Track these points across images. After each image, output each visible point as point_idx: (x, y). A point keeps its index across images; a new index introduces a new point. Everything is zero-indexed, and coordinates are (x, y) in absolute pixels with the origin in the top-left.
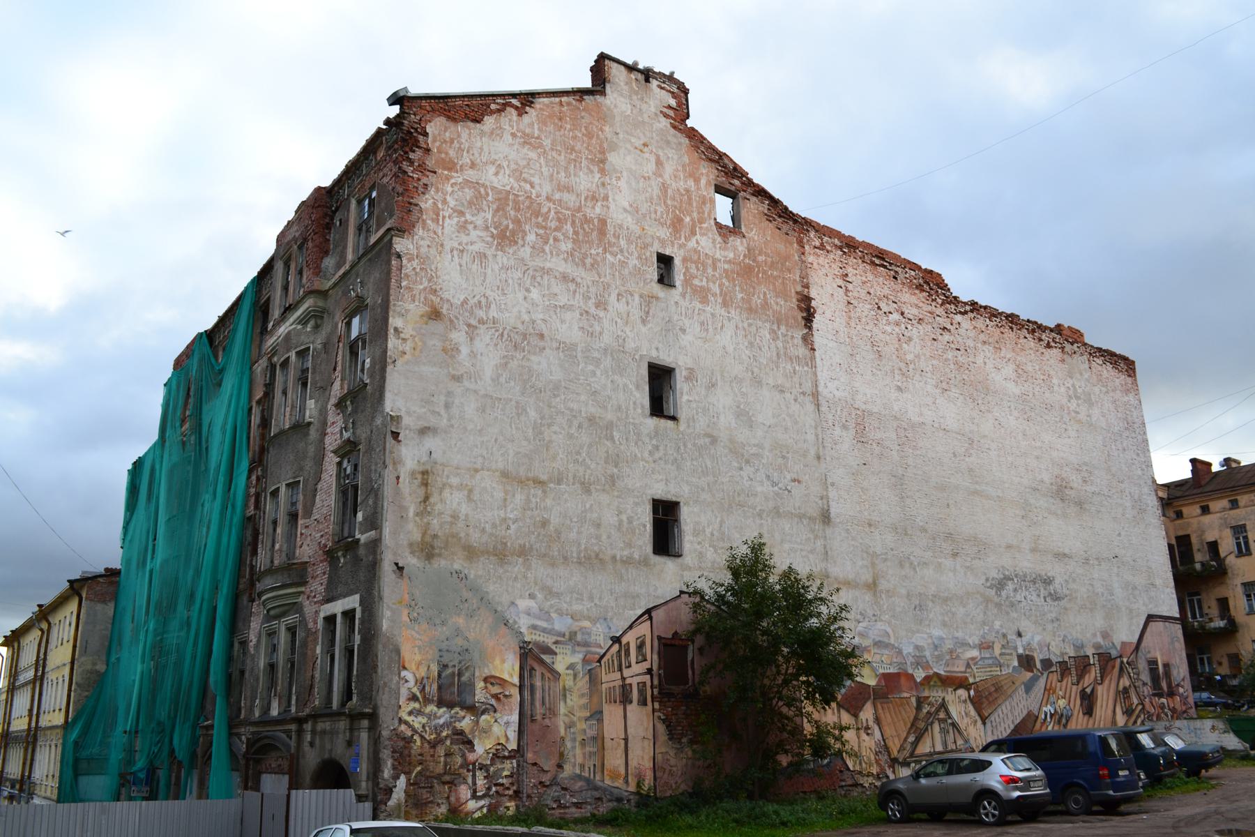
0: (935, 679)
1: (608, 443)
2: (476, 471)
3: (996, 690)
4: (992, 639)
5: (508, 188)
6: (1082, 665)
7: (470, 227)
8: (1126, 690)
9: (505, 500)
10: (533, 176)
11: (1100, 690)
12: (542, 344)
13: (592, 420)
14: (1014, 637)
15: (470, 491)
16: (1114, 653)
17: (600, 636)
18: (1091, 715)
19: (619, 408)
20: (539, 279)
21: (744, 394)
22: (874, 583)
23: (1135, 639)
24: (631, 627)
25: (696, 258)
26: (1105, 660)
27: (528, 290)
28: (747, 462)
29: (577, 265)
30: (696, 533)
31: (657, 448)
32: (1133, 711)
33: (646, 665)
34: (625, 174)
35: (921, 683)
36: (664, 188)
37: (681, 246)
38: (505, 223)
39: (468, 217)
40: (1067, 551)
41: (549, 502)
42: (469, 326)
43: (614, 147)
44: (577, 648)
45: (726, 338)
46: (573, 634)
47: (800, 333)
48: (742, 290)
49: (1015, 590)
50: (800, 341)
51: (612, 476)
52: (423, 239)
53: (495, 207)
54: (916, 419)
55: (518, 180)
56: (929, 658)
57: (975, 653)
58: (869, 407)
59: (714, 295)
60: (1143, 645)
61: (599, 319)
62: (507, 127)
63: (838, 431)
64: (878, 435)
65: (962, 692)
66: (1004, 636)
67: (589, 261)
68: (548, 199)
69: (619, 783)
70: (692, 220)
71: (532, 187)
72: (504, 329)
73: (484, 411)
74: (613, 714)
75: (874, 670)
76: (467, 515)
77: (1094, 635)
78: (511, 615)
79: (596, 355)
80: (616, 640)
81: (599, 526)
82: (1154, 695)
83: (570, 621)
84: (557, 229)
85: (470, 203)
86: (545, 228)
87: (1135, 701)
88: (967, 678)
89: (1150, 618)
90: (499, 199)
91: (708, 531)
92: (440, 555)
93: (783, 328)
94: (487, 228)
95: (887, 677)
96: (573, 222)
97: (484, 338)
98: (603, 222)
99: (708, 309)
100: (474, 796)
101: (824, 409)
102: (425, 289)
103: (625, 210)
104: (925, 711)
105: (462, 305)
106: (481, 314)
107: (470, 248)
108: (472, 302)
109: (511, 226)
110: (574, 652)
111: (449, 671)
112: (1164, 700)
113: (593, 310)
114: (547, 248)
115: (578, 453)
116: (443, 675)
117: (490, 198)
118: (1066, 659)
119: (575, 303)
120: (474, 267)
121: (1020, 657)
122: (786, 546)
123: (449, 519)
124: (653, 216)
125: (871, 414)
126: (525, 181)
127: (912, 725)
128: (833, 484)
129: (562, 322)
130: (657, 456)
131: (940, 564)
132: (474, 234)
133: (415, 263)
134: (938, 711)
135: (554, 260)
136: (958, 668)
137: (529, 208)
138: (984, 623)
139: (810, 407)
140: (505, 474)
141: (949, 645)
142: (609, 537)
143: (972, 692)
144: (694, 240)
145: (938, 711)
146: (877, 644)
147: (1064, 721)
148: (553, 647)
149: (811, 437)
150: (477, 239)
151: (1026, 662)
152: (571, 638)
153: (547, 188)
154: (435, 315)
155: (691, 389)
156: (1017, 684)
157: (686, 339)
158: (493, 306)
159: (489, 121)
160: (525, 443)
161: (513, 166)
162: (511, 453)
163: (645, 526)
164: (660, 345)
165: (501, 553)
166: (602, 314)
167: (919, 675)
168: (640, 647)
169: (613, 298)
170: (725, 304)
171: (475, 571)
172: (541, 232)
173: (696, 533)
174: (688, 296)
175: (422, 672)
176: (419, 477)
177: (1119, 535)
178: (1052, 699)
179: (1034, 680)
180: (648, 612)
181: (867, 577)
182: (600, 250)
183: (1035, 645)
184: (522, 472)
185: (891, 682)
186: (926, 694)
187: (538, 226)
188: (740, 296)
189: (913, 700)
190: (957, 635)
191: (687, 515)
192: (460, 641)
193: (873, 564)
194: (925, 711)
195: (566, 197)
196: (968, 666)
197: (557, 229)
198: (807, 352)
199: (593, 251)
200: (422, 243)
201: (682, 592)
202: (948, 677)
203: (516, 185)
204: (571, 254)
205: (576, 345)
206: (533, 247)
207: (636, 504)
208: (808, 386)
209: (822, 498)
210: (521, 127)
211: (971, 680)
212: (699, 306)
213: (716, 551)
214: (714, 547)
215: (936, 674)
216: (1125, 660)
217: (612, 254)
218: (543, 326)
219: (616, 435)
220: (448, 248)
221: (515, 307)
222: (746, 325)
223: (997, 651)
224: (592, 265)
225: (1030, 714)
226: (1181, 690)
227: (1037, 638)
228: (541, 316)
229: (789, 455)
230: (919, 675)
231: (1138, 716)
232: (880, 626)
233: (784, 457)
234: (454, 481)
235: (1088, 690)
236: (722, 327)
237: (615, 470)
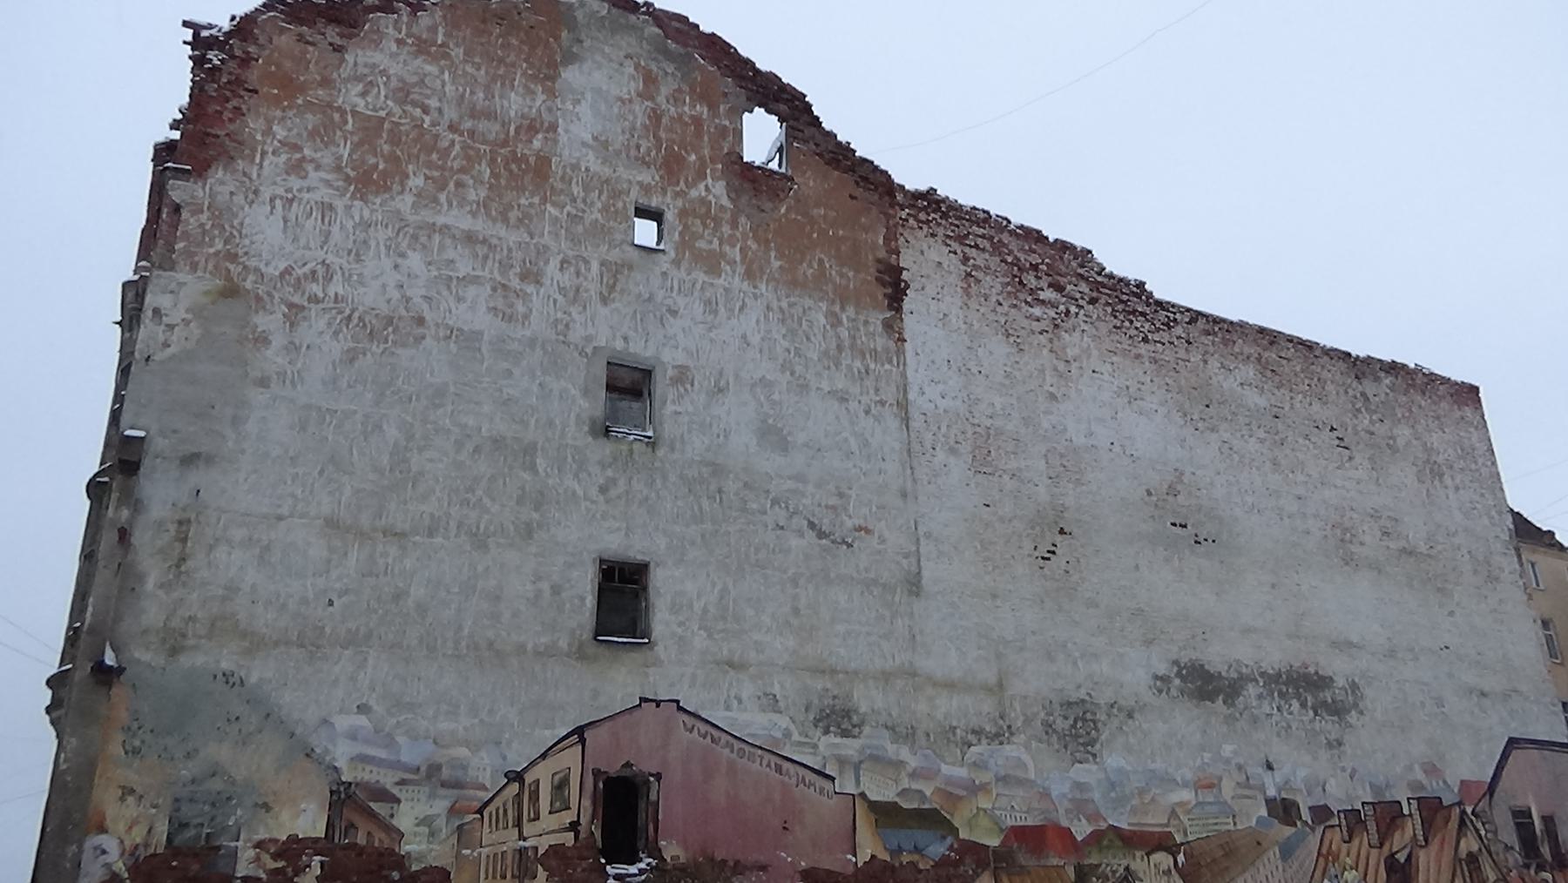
0: (1111, 835)
1: (526, 476)
2: (280, 518)
3: (1226, 855)
5: (383, 114)
6: (1388, 815)
7: (310, 168)
8: (1472, 858)
9: (329, 561)
10: (428, 97)
12: (421, 330)
13: (498, 442)
14: (1260, 770)
15: (267, 548)
17: (485, 769)
19: (551, 423)
20: (423, 239)
21: (774, 403)
22: (1000, 685)
24: (544, 756)
25: (703, 210)
27: (403, 255)
28: (775, 502)
29: (494, 220)
31: (614, 481)
33: (568, 817)
34: (589, 96)
36: (656, 116)
37: (677, 195)
38: (372, 161)
39: (307, 152)
41: (408, 563)
42: (291, 306)
43: (570, 58)
44: (443, 792)
45: (749, 322)
46: (434, 769)
47: (877, 318)
48: (780, 256)
49: (1260, 697)
50: (880, 329)
51: (528, 525)
52: (222, 183)
53: (356, 139)
54: (1080, 440)
55: (402, 102)
57: (1186, 795)
58: (998, 423)
59: (732, 263)
61: (524, 296)
62: (391, 31)
63: (941, 456)
64: (1013, 464)
65: (1162, 859)
66: (1240, 768)
67: (514, 215)
68: (452, 128)
70: (701, 159)
71: (426, 111)
72: (353, 311)
73: (303, 428)
76: (253, 586)
77: (1410, 768)
78: (319, 742)
79: (515, 346)
80: (516, 777)
81: (498, 598)
83: (429, 747)
84: (462, 170)
85: (313, 134)
86: (442, 168)
89: (1513, 743)
90: (366, 129)
91: (698, 606)
92: (196, 648)
93: (851, 311)
94: (338, 169)
96: (493, 161)
97: (316, 324)
98: (544, 162)
99: (721, 281)
101: (917, 423)
102: (217, 253)
103: (584, 144)
105: (282, 275)
106: (316, 289)
107: (306, 196)
108: (300, 272)
109: (381, 167)
110: (432, 796)
111: (191, 833)
113: (515, 283)
114: (443, 197)
115: (471, 490)
116: (177, 841)
117: (349, 127)
119: (486, 273)
120: (309, 224)
121: (1270, 802)
122: (840, 628)
123: (221, 592)
124: (633, 153)
125: (1000, 432)
126: (415, 104)
128: (928, 535)
129: (459, 299)
130: (613, 493)
132: (314, 176)
133: (204, 217)
135: (455, 212)
136: (1154, 821)
137: (415, 141)
139: (893, 423)
140: (332, 523)
142: (515, 615)
143: (1181, 858)
144: (702, 186)
146: (1003, 779)
148: (395, 791)
150: (318, 185)
151: (1284, 810)
152: (432, 775)
153: (451, 114)
154: (231, 291)
155: (681, 396)
157: (675, 326)
158: (338, 277)
160: (372, 476)
161: (394, 83)
162: (348, 491)
163: (583, 599)
164: (631, 334)
165: (310, 642)
166: (530, 289)
167: (1081, 830)
168: (561, 786)
169: (554, 263)
170: (749, 275)
171: (258, 672)
172: (436, 174)
173: (675, 609)
174: (685, 265)
175: (138, 835)
176: (173, 528)
180: (579, 732)
181: (990, 677)
182: (536, 200)
183: (1298, 783)
184: (365, 520)
186: (1093, 860)
187: (430, 165)
188: (776, 264)
189: (1071, 872)
190: (1153, 766)
191: (659, 580)
192: (216, 785)
193: (999, 656)
195: (482, 125)
196: (1173, 814)
197: (462, 170)
198: (891, 344)
199: (523, 201)
200: (219, 189)
201: (643, 700)
203: (397, 110)
204: (485, 205)
205: (481, 333)
206: (418, 195)
207: (570, 566)
208: (890, 394)
209: (906, 556)
210: (414, 30)
212: (701, 277)
213: (710, 636)
214: (706, 629)
216: (1469, 810)
217: (554, 204)
218: (425, 306)
219: (541, 463)
220: (266, 194)
221: (378, 283)
222: (784, 304)
223: (1228, 789)
224: (520, 220)
227: (1302, 773)
228: (423, 292)
229: (853, 493)
230: (1081, 830)
233: (841, 495)
234: (238, 534)
235: (1402, 857)
236: (741, 309)
237: (535, 516)
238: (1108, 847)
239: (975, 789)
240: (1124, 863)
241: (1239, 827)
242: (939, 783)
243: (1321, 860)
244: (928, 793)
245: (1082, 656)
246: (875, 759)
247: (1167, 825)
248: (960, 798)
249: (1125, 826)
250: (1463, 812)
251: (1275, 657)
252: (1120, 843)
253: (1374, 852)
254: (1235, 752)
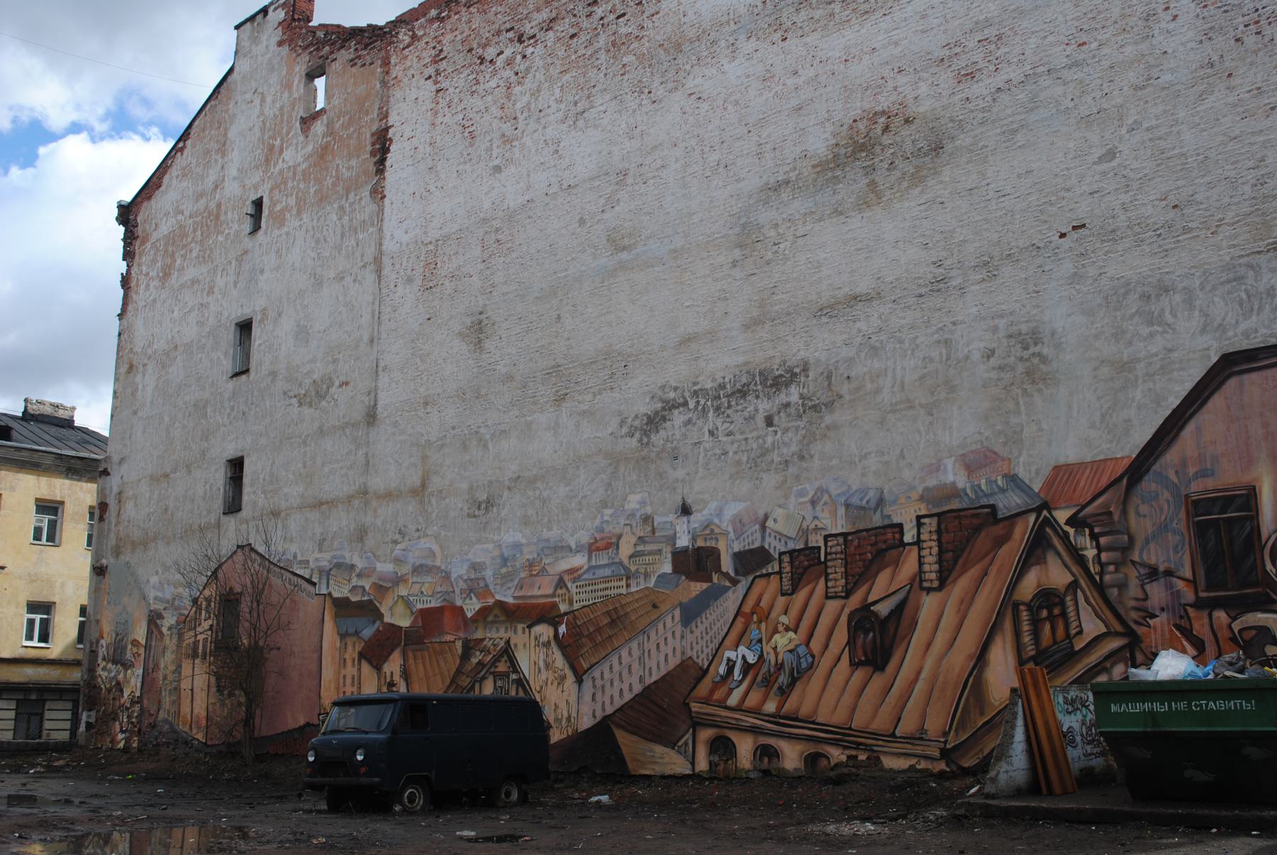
0: (496, 611)
3: (613, 623)
4: (617, 531)
6: (872, 546)
14: (671, 517)
16: (1009, 502)
30: (252, 485)
32: (1072, 656)
35: (475, 619)
40: (863, 287)
56: (490, 580)
57: (579, 560)
60: (1171, 457)
65: (544, 631)
66: (647, 519)
69: (186, 729)
74: (186, 669)
75: (408, 604)
87: (1092, 626)
88: (555, 605)
89: (1231, 365)
91: (261, 477)
95: (425, 614)
100: (122, 732)
104: (474, 661)
118: (816, 540)
127: (452, 682)
131: (529, 425)
134: (497, 659)
136: (541, 590)
138: (604, 504)
139: (370, 277)
141: (529, 554)
143: (562, 629)
145: (497, 659)
147: (783, 679)
149: (366, 319)
151: (696, 562)
156: (663, 608)
159: (166, 179)
167: (472, 607)
178: (754, 633)
179: (714, 594)
185: (430, 620)
186: (479, 635)
189: (459, 644)
190: (546, 534)
193: (424, 458)
194: (474, 661)
196: (561, 583)
202: (518, 606)
211: (563, 608)
215: (500, 604)
216: (1062, 516)
223: (626, 549)
227: (732, 510)
230: (472, 607)
232: (425, 543)
235: (883, 609)
238: (493, 622)
239: (399, 580)
240: (506, 636)
241: (633, 589)
242: (374, 579)
243: (740, 620)
244: (367, 588)
245: (493, 436)
246: (338, 566)
247: (553, 595)
248: (387, 589)
249: (511, 600)
250: (1050, 522)
251: (722, 363)
252: (503, 618)
253: (832, 606)
254: (643, 503)
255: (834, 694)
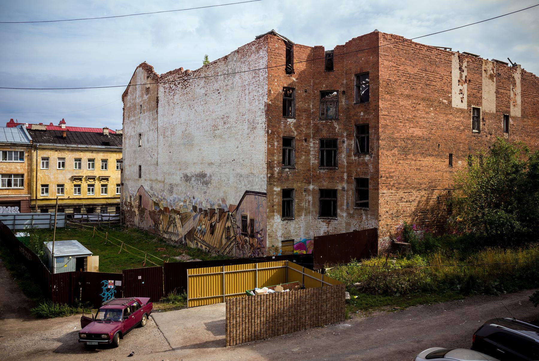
6: (212, 212)
11: (218, 225)
16: (226, 210)
18: (213, 235)
23: (237, 204)
26: (222, 212)
32: (230, 239)
57: (182, 204)
60: (240, 207)
82: (242, 234)
87: (232, 234)
89: (247, 193)
112: (247, 238)
121: (193, 206)
177: (238, 147)
178: (201, 224)
179: (196, 216)
183: (198, 203)
216: (230, 213)
225: (193, 228)
226: (259, 236)
230: (170, 209)
231: (232, 242)
235: (213, 224)
250: (229, 214)
251: (198, 170)
255: (207, 238)
